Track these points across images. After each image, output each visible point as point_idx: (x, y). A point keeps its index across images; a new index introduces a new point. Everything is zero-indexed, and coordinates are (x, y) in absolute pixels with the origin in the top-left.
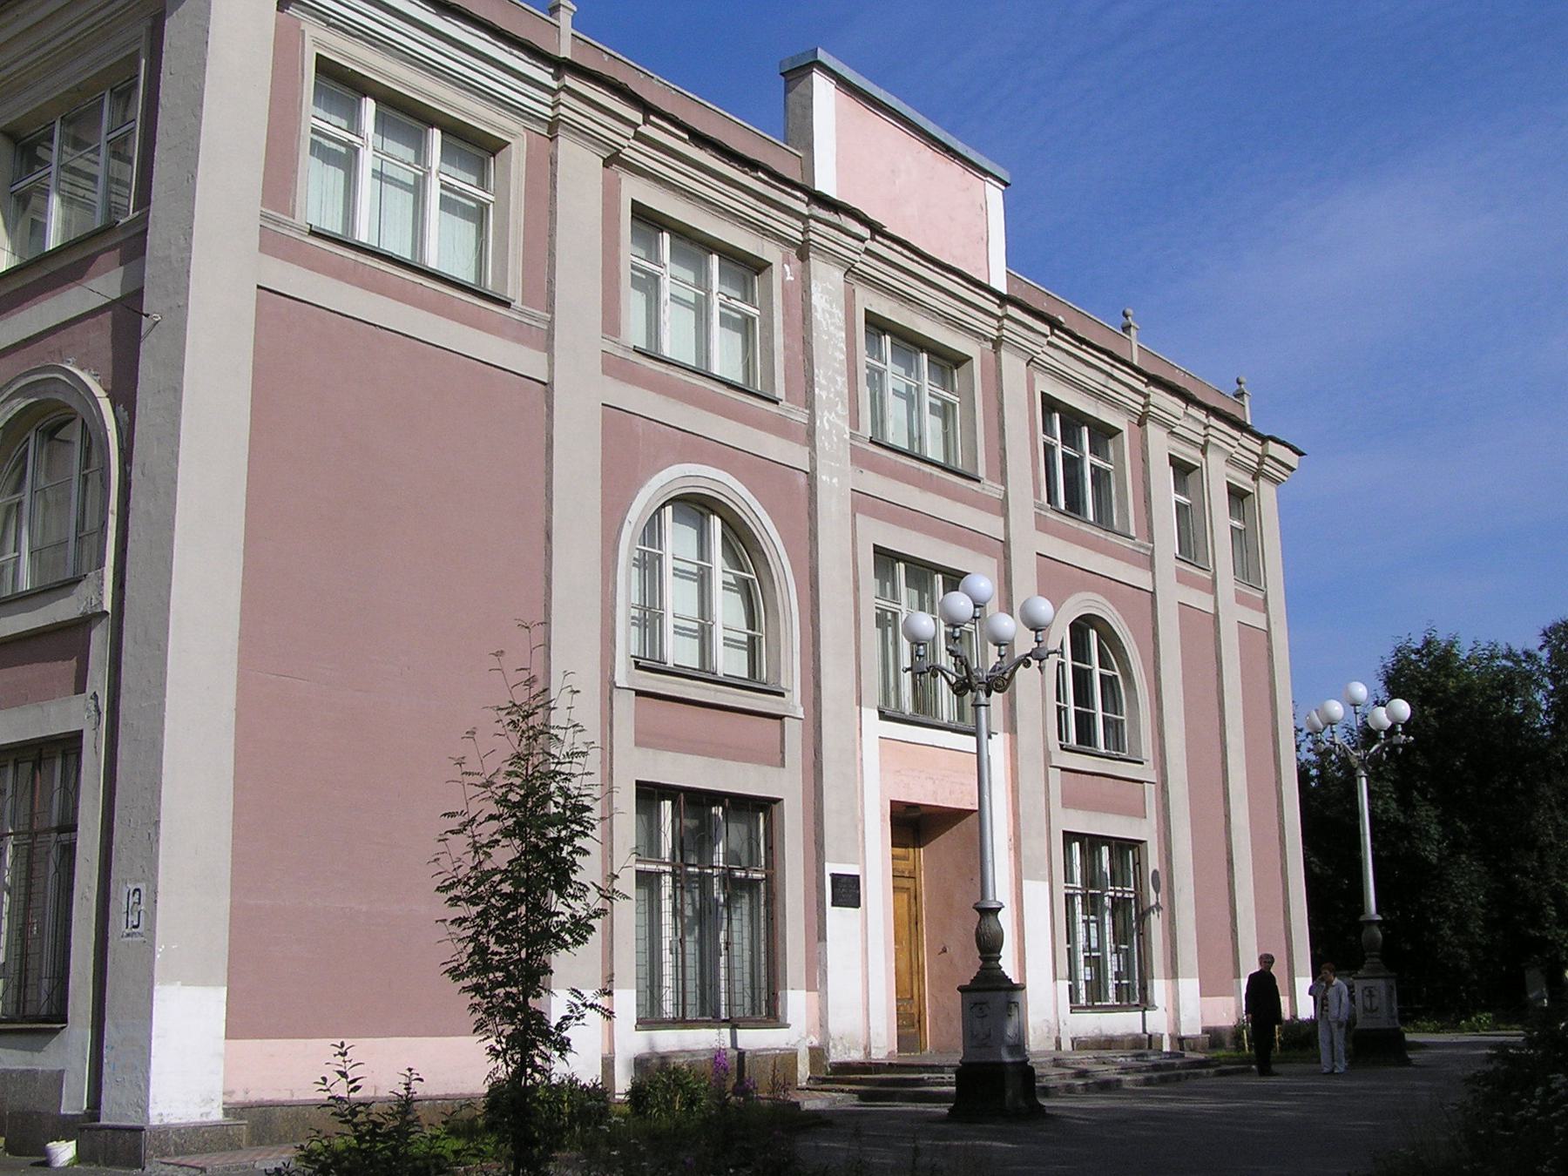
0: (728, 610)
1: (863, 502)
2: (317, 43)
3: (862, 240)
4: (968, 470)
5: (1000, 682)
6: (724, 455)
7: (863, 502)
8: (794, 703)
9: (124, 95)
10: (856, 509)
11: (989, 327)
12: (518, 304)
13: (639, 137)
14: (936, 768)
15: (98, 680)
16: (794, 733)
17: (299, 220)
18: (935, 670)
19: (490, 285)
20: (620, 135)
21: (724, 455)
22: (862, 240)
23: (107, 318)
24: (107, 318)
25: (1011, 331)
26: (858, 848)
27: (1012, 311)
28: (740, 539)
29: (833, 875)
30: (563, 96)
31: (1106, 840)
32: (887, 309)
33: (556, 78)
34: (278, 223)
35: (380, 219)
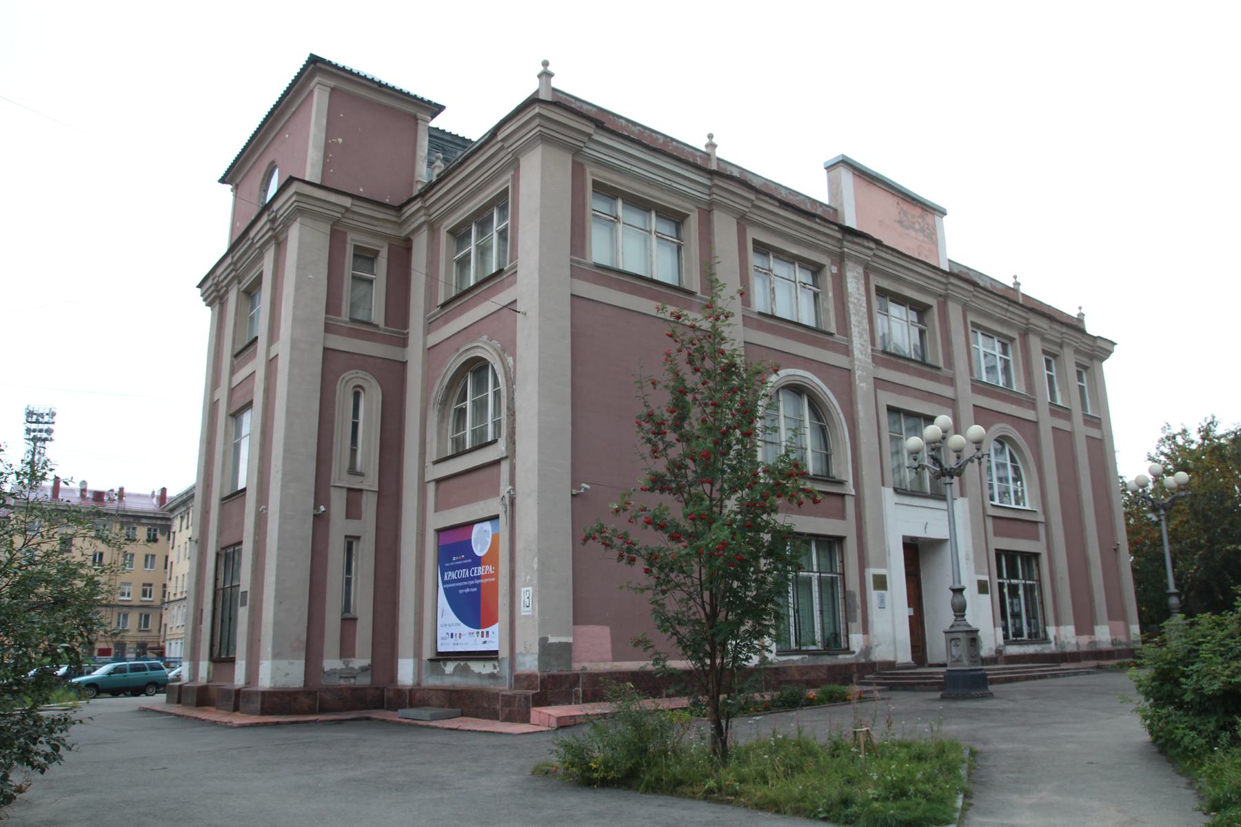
0: (809, 439)
1: (879, 383)
2: (592, 174)
3: (871, 249)
4: (934, 364)
5: (958, 472)
6: (806, 363)
7: (879, 383)
8: (850, 489)
9: (503, 209)
10: (876, 387)
11: (939, 289)
12: (699, 294)
13: (755, 206)
14: (924, 520)
15: (505, 488)
16: (850, 504)
17: (588, 261)
18: (923, 467)
19: (685, 285)
20: (743, 206)
21: (806, 363)
22: (871, 249)
23: (879, 391)
24: (879, 391)
25: (952, 291)
26: (883, 563)
27: (953, 280)
28: (817, 408)
29: (875, 576)
30: (714, 190)
31: (1022, 554)
32: (885, 284)
33: (711, 180)
34: (579, 263)
35: (632, 261)
